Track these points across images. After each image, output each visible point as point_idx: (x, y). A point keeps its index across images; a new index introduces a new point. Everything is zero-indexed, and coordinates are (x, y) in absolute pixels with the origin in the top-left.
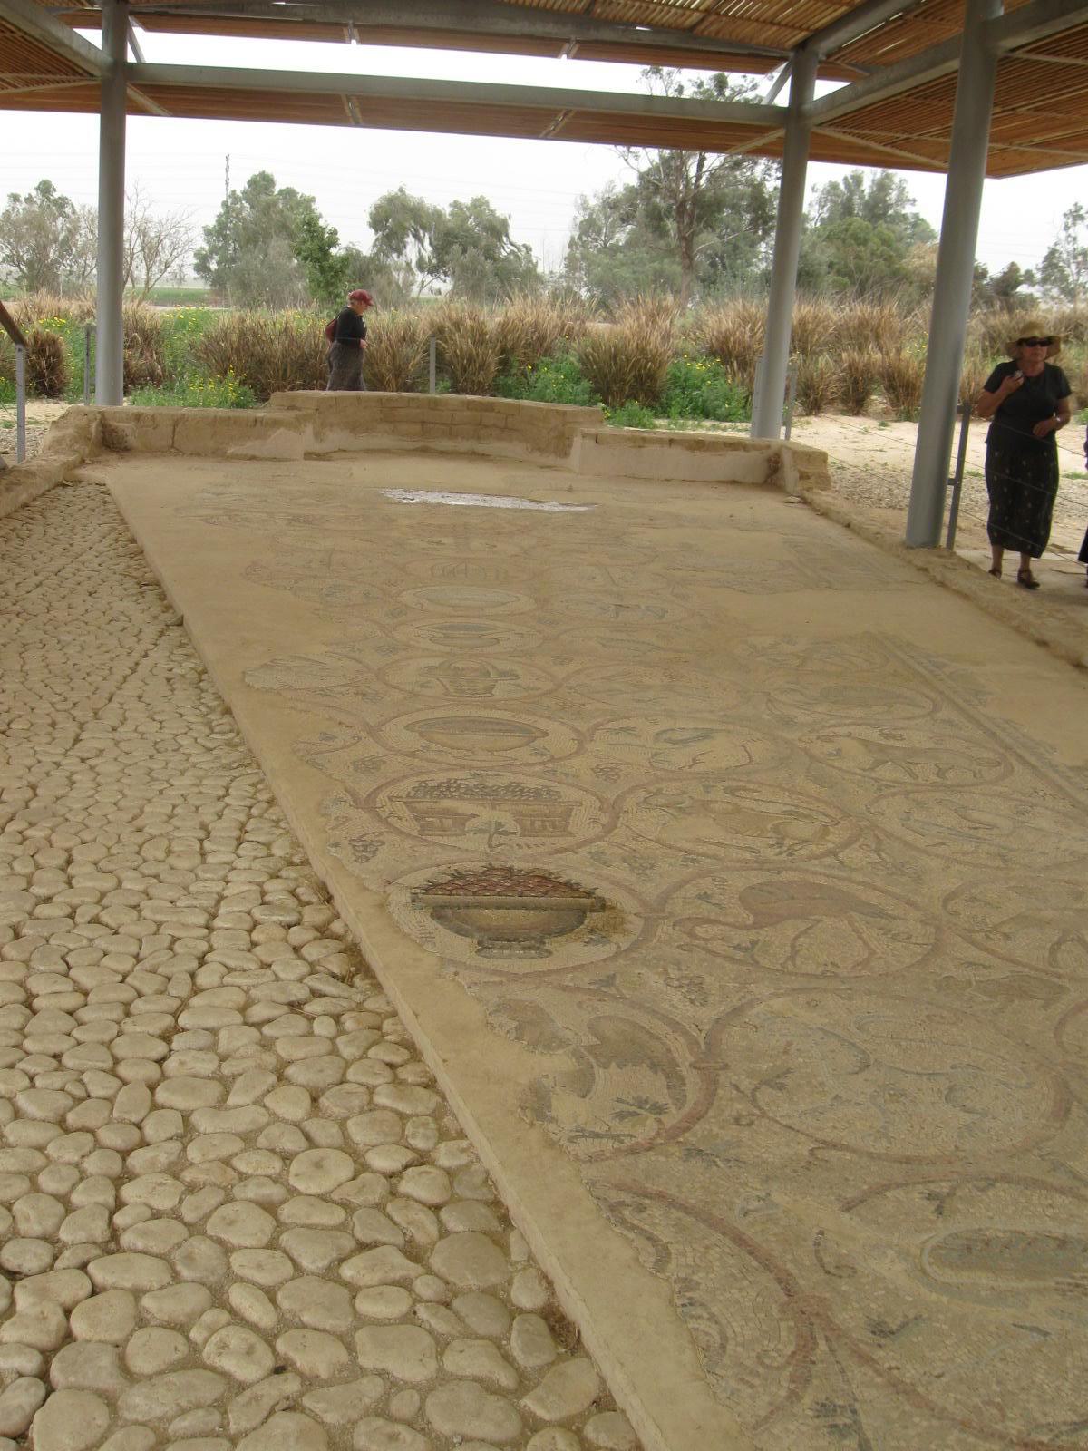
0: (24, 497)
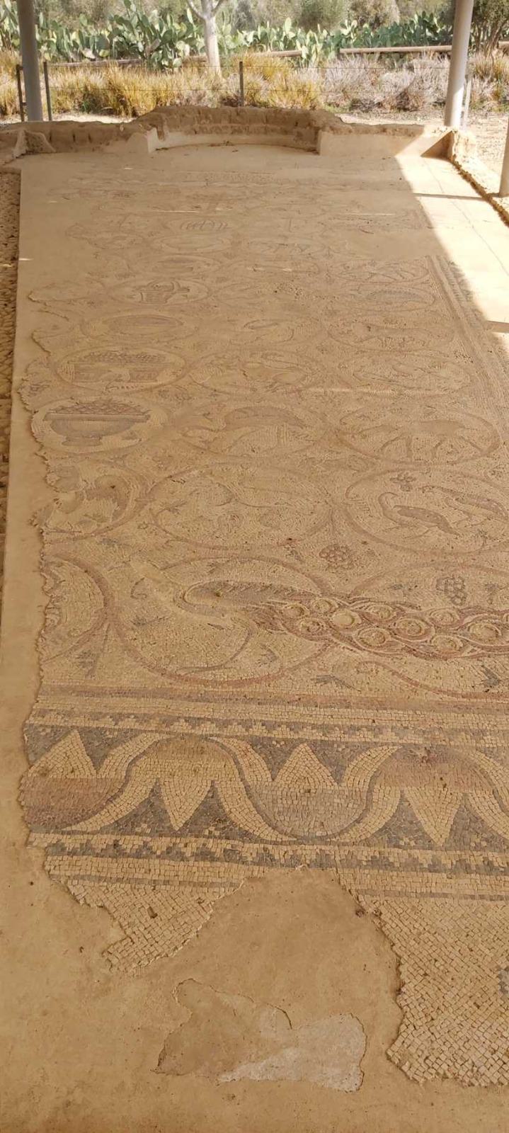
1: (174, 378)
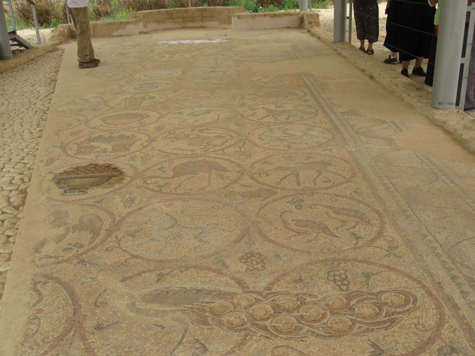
0: (33, 56)
1: (141, 147)
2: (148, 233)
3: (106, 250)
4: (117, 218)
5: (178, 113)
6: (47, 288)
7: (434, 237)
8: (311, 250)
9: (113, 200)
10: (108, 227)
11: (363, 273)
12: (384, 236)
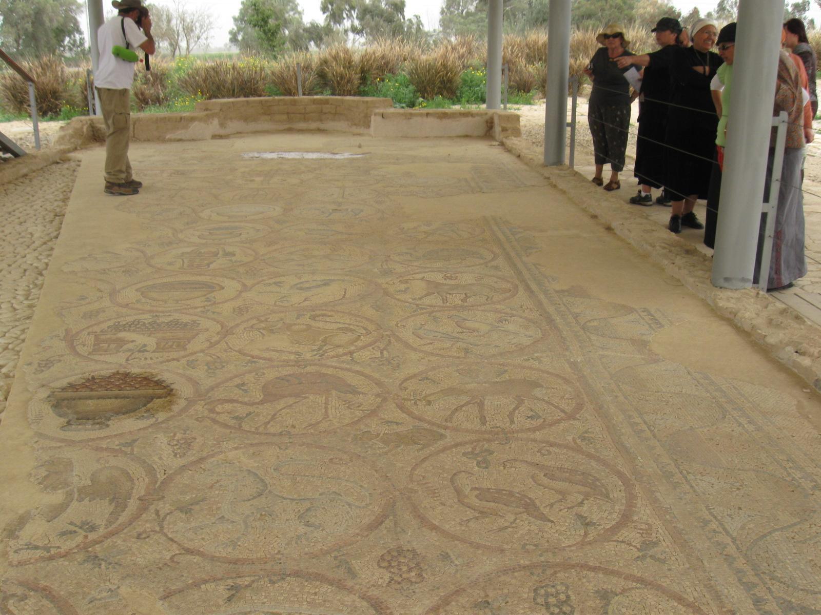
0: (25, 171)
1: (207, 344)
2: (214, 507)
3: (139, 537)
4: (159, 476)
5: (275, 283)
6: (27, 607)
7: (721, 524)
8: (505, 546)
9: (154, 441)
10: (143, 493)
11: (597, 592)
12: (633, 522)
